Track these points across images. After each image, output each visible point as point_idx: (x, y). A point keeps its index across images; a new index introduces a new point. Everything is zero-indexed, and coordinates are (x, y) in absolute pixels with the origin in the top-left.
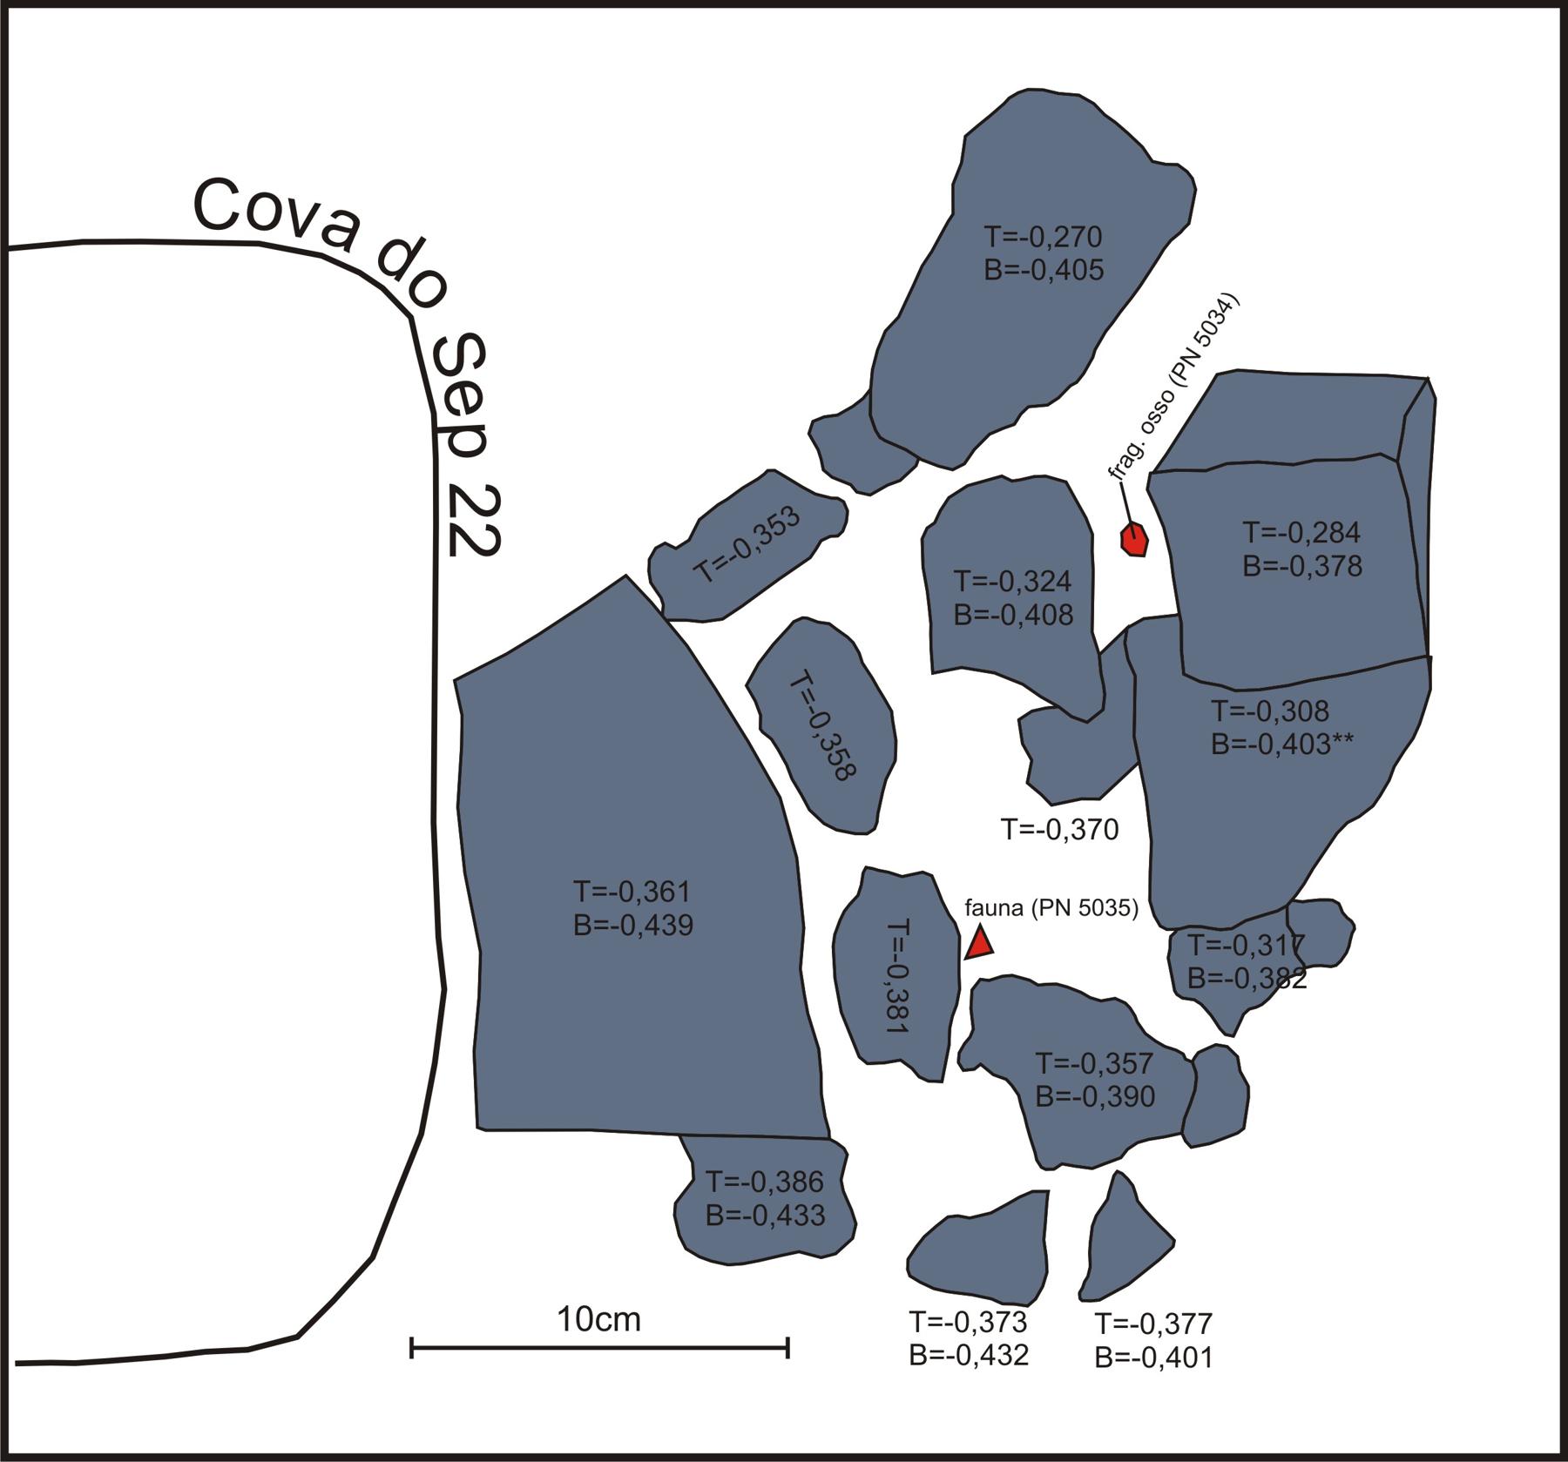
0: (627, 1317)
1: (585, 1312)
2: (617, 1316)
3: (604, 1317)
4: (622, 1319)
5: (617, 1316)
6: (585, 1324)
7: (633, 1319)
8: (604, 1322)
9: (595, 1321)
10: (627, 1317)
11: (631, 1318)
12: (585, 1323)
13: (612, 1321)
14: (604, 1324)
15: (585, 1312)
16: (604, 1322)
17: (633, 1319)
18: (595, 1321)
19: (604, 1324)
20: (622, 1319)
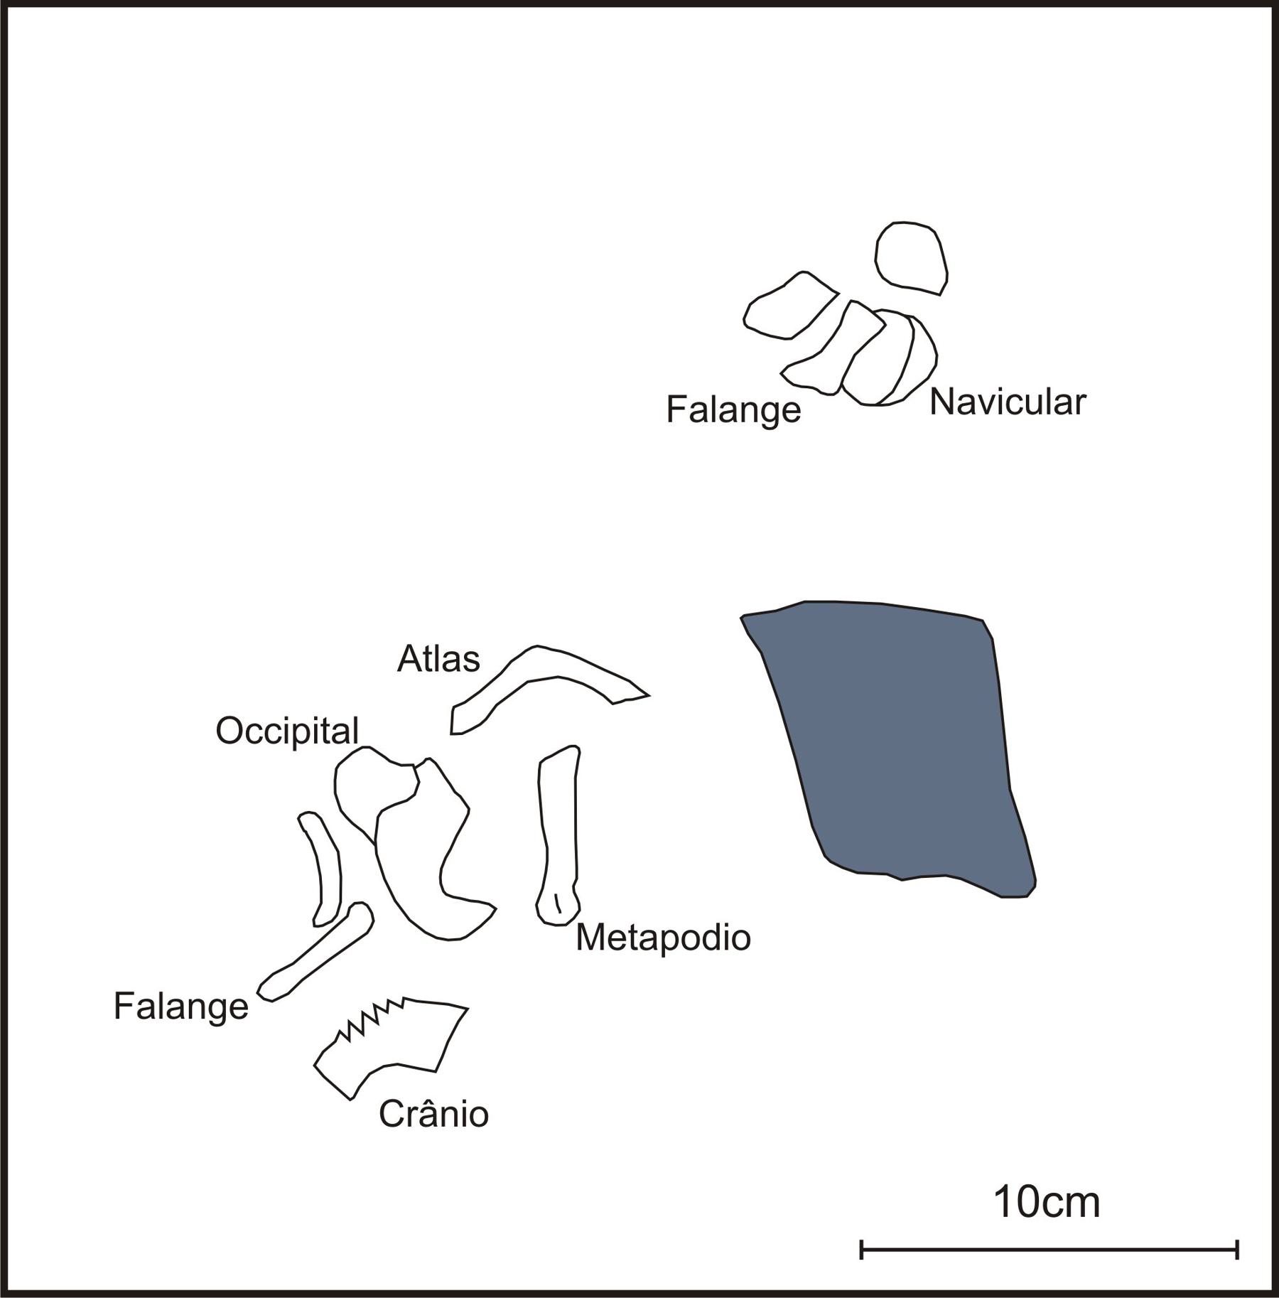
0: (1083, 1199)
1: (1029, 1194)
2: (1070, 1197)
3: (1053, 1200)
4: (1076, 1202)
5: (1070, 1197)
6: (1028, 1208)
7: (1090, 1202)
8: (1054, 1205)
9: (1042, 1204)
10: (1083, 1199)
11: (1087, 1201)
12: (1028, 1206)
13: (1063, 1204)
15: (1029, 1194)
16: (1054, 1205)
17: (1090, 1202)
18: (1042, 1204)
20: (1076, 1202)
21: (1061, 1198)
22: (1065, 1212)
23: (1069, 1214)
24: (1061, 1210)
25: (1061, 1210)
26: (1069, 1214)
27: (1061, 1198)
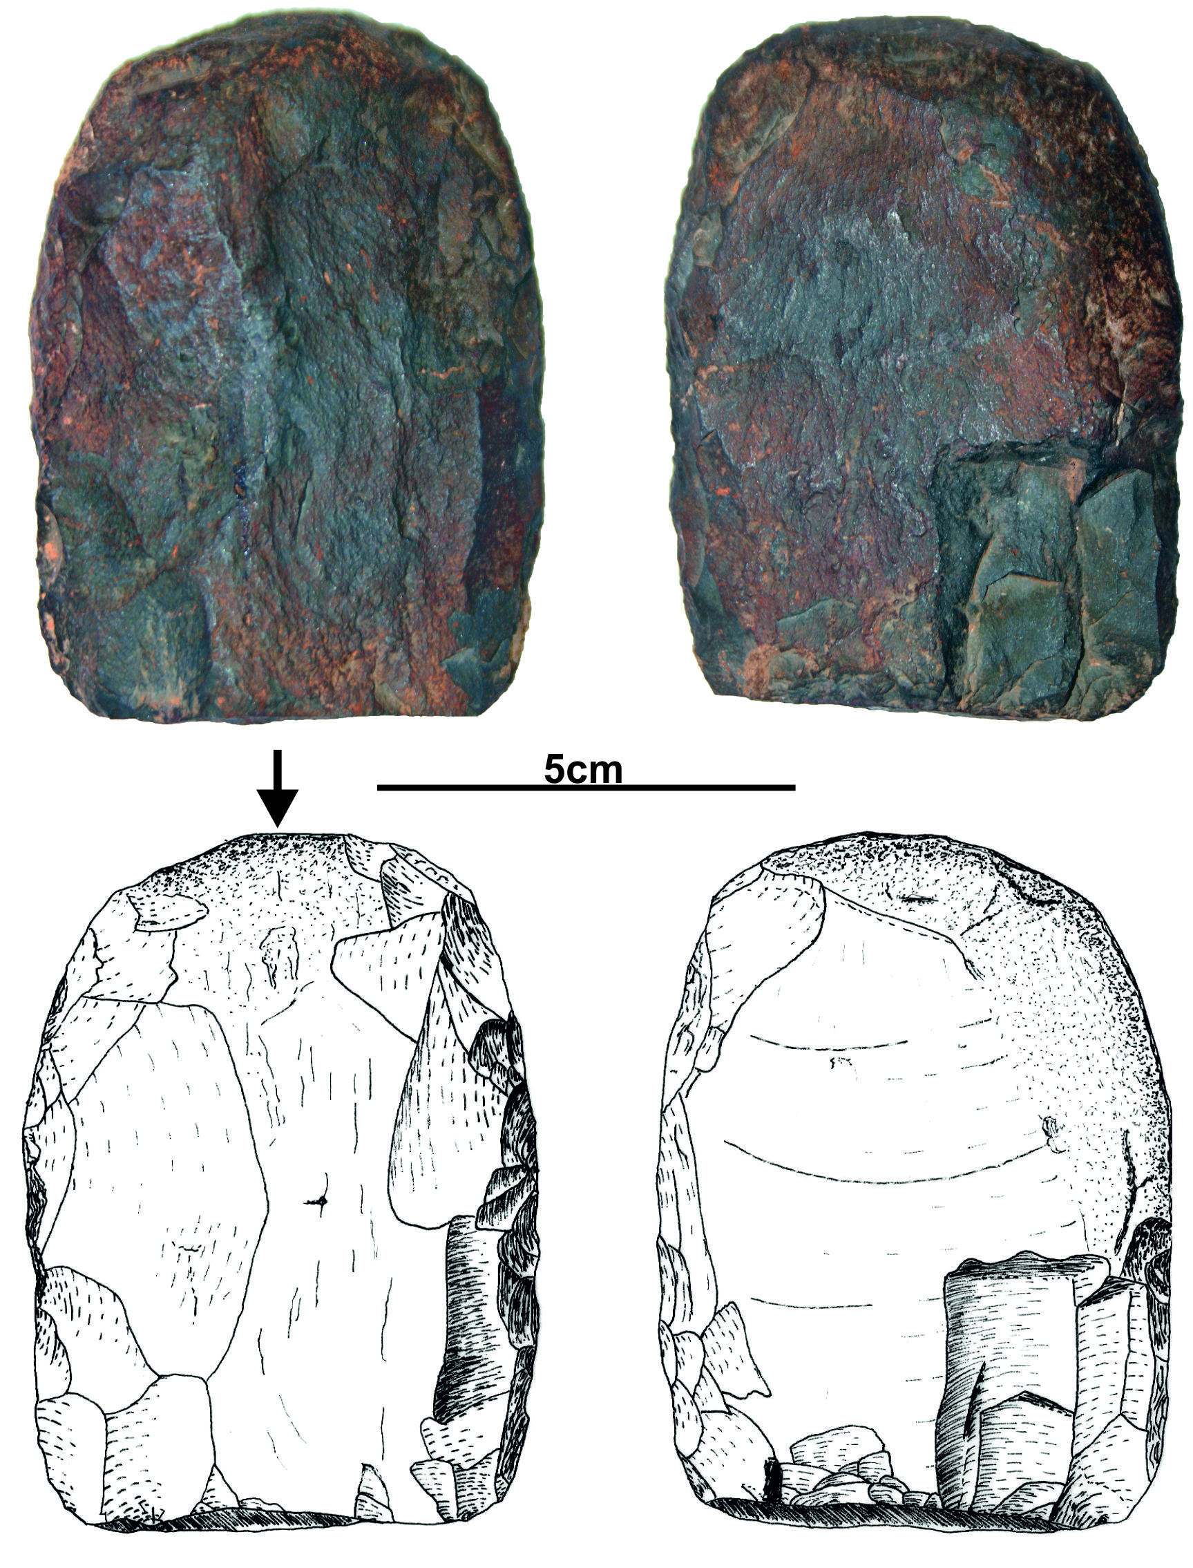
4: (600, 770)
5: (594, 766)
7: (613, 770)
13: (587, 772)
17: (613, 770)
20: (600, 770)
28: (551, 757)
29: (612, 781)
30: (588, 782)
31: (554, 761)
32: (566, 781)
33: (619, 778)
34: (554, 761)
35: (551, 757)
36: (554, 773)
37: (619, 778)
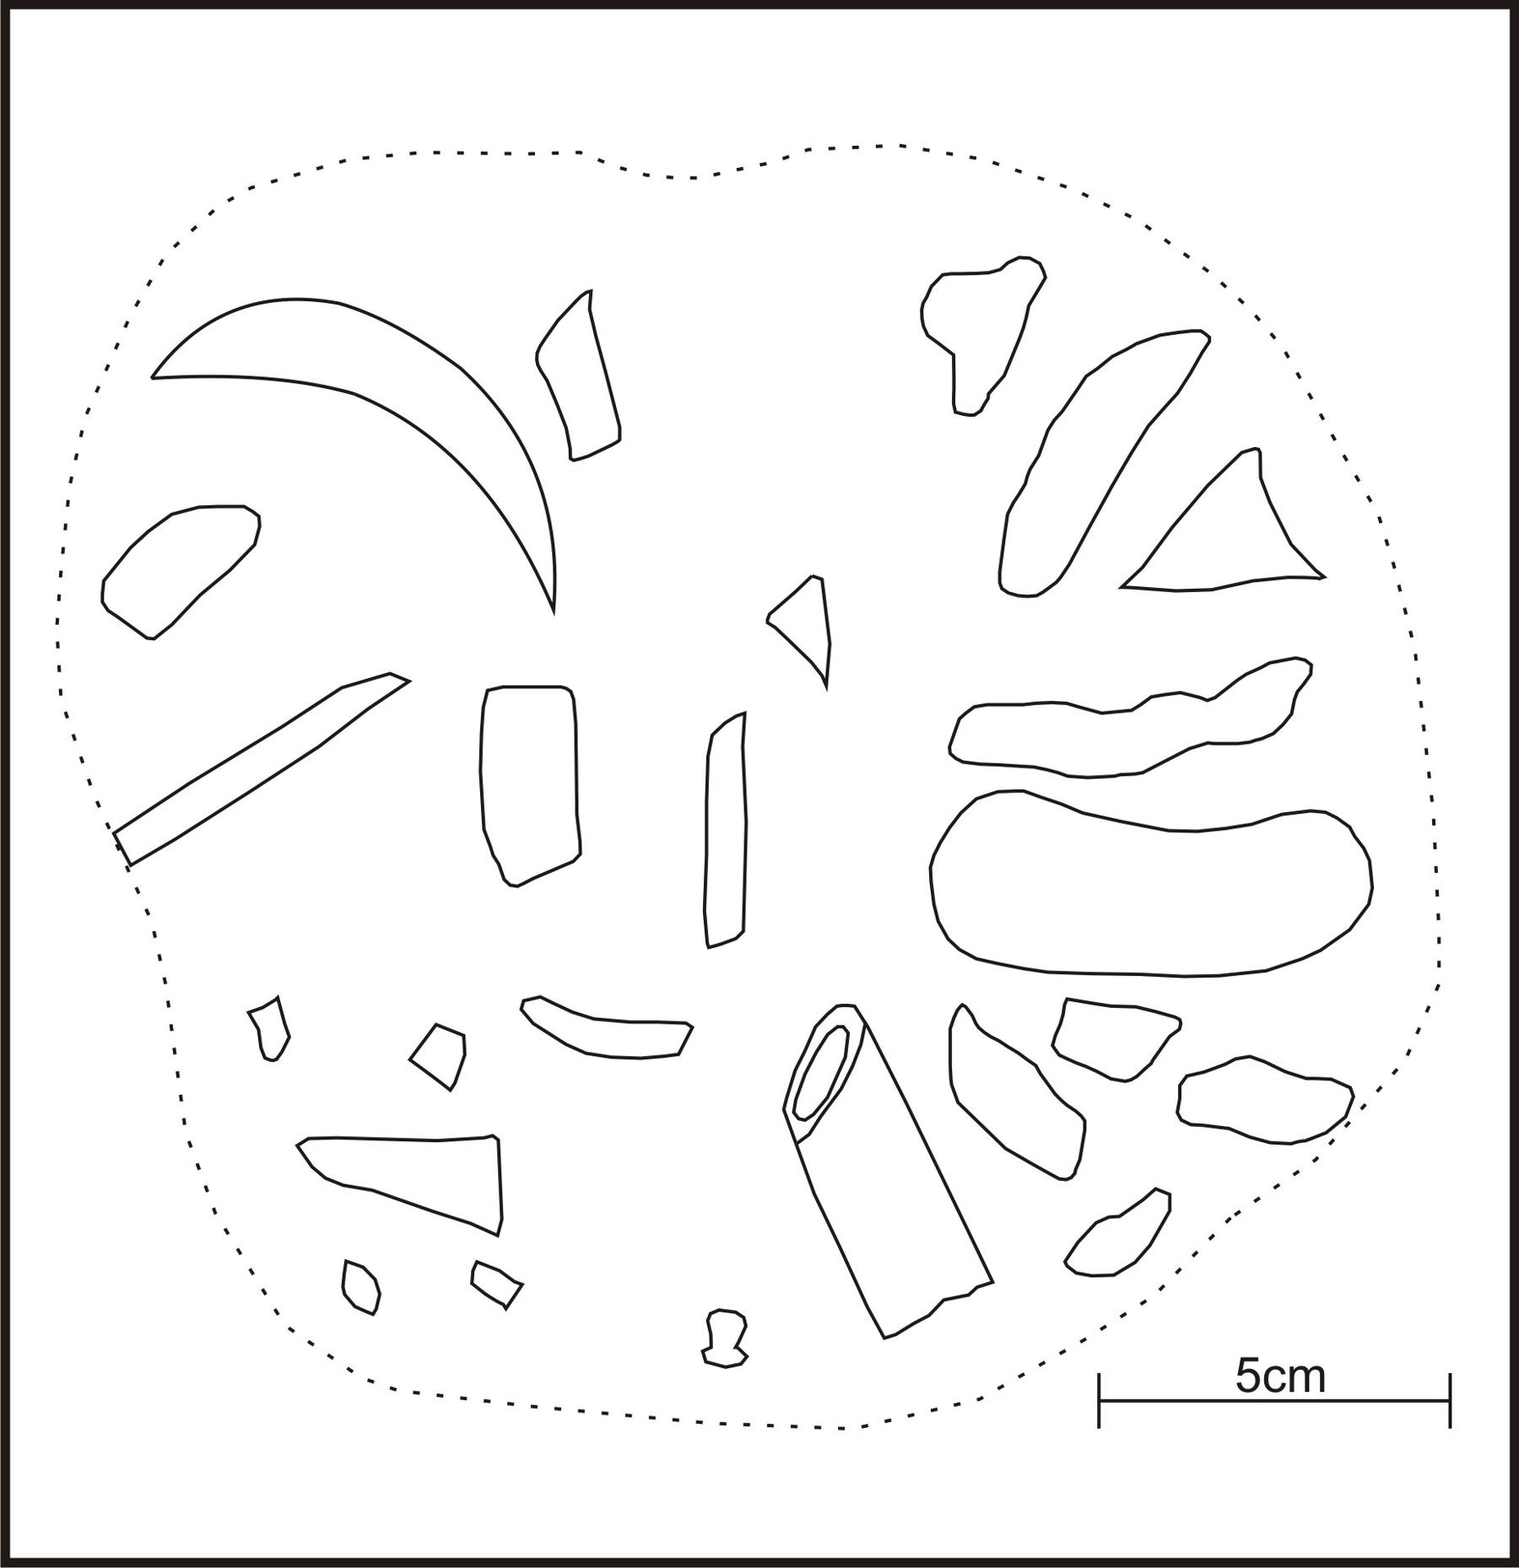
0: (1307, 1372)
2: (1293, 1371)
3: (1274, 1374)
4: (1300, 1376)
5: (1293, 1371)
7: (1315, 1376)
8: (1276, 1379)
10: (1307, 1372)
13: (1286, 1379)
14: (1274, 1384)
16: (1276, 1379)
17: (1315, 1376)
19: (1275, 1386)
20: (1300, 1376)
21: (1283, 1372)
22: (1288, 1387)
23: (1292, 1389)
24: (1283, 1385)
25: (1283, 1385)
26: (1292, 1389)
27: (1283, 1372)
28: (1243, 1360)
29: (1314, 1393)
30: (1286, 1394)
31: (1247, 1365)
32: (1262, 1392)
33: (1322, 1389)
34: (1247, 1365)
35: (1243, 1360)
36: (1248, 1381)
37: (1322, 1389)
